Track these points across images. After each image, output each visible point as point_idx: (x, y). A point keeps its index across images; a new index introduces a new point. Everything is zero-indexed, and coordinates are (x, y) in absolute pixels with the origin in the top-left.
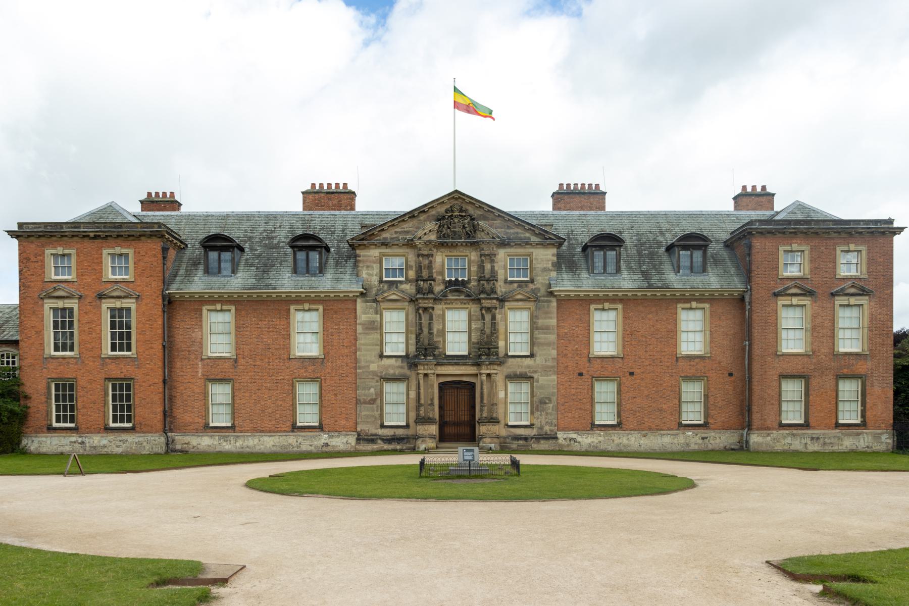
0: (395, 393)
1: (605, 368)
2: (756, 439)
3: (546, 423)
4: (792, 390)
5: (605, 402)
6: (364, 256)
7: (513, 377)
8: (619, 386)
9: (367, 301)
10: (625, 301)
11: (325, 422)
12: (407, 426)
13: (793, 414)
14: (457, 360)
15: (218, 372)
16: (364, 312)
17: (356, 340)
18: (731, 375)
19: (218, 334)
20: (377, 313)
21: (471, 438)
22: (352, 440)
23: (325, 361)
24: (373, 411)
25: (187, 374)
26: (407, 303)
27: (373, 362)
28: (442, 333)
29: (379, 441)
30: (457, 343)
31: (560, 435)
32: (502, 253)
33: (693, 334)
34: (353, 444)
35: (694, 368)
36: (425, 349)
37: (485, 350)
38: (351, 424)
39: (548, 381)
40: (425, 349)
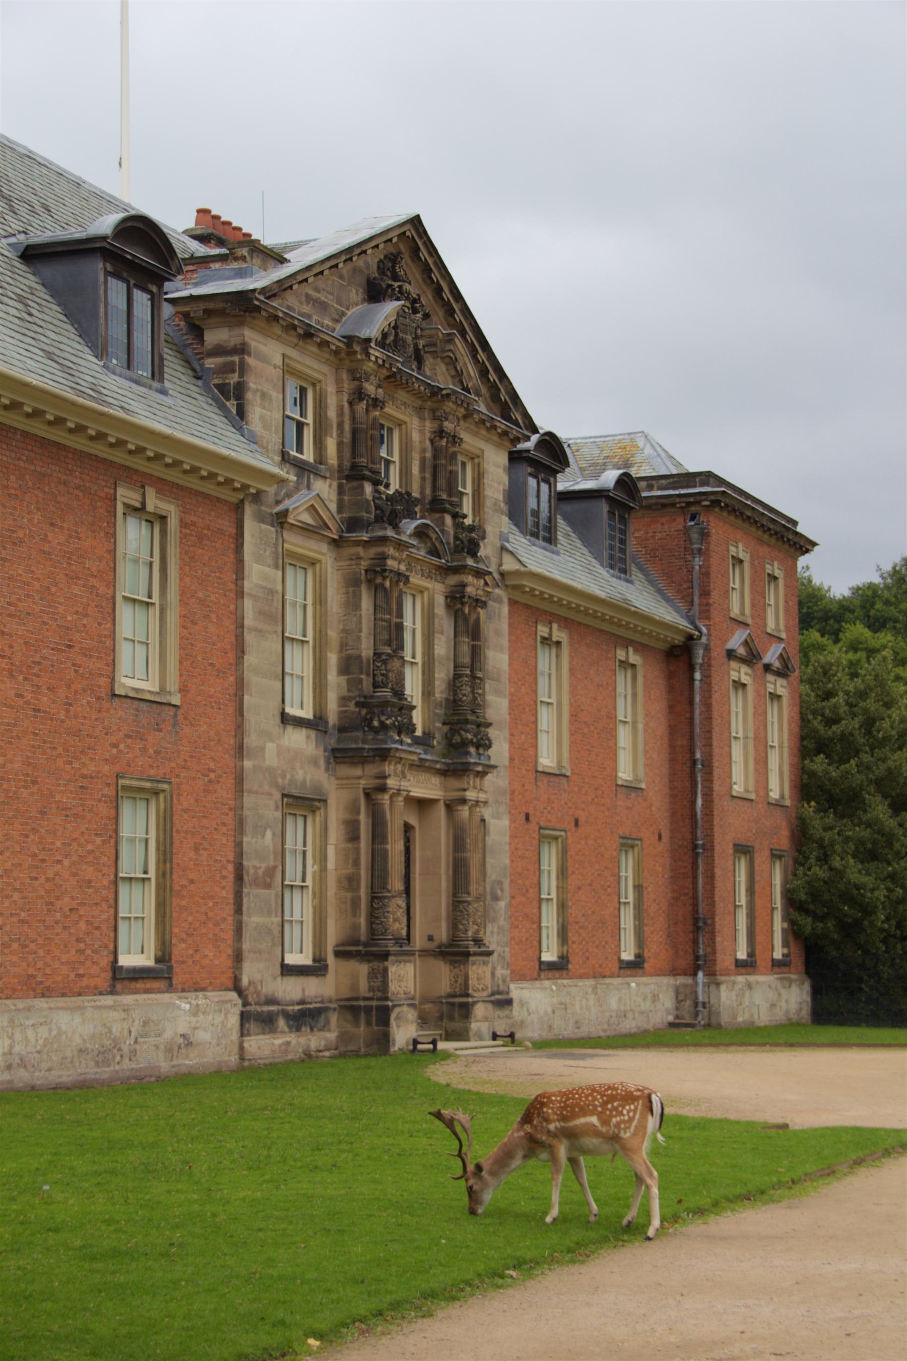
6: (260, 357)
8: (564, 854)
9: (263, 522)
11: (179, 950)
12: (318, 969)
17: (240, 649)
18: (660, 838)
20: (277, 567)
22: (234, 1020)
23: (180, 711)
24: (269, 914)
26: (324, 547)
27: (270, 738)
29: (282, 1023)
31: (517, 991)
34: (235, 1036)
38: (224, 961)
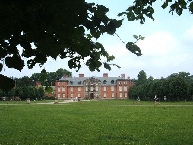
0: (87, 94)
1: (105, 92)
2: (117, 98)
3: (99, 97)
4: (121, 94)
5: (105, 95)
7: (97, 93)
10: (107, 86)
13: (121, 96)
14: (92, 92)
15: (72, 93)
16: (84, 87)
19: (72, 90)
21: (93, 98)
25: (69, 93)
28: (91, 89)
30: (92, 90)
32: (96, 83)
33: (113, 89)
35: (113, 92)
36: (89, 91)
37: (94, 91)
39: (100, 93)
40: (89, 91)
